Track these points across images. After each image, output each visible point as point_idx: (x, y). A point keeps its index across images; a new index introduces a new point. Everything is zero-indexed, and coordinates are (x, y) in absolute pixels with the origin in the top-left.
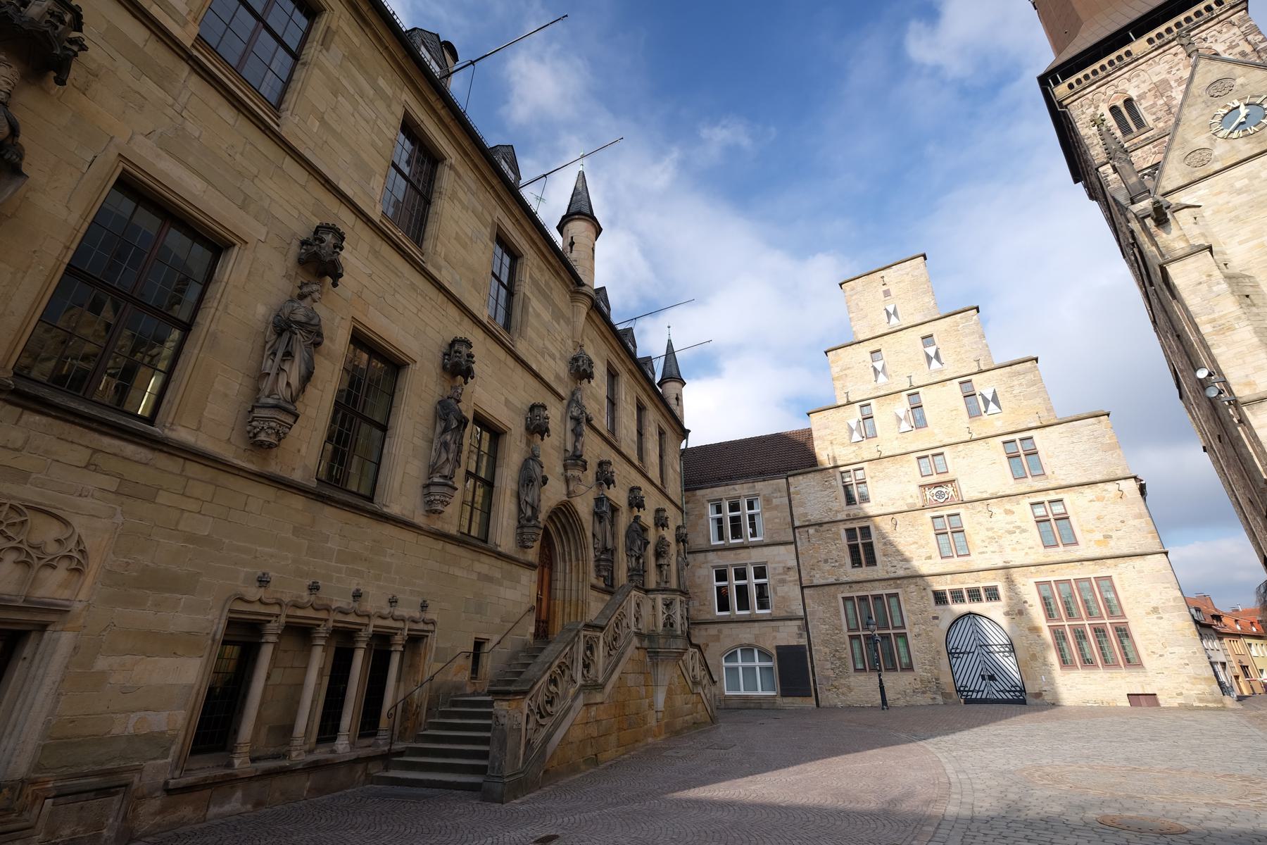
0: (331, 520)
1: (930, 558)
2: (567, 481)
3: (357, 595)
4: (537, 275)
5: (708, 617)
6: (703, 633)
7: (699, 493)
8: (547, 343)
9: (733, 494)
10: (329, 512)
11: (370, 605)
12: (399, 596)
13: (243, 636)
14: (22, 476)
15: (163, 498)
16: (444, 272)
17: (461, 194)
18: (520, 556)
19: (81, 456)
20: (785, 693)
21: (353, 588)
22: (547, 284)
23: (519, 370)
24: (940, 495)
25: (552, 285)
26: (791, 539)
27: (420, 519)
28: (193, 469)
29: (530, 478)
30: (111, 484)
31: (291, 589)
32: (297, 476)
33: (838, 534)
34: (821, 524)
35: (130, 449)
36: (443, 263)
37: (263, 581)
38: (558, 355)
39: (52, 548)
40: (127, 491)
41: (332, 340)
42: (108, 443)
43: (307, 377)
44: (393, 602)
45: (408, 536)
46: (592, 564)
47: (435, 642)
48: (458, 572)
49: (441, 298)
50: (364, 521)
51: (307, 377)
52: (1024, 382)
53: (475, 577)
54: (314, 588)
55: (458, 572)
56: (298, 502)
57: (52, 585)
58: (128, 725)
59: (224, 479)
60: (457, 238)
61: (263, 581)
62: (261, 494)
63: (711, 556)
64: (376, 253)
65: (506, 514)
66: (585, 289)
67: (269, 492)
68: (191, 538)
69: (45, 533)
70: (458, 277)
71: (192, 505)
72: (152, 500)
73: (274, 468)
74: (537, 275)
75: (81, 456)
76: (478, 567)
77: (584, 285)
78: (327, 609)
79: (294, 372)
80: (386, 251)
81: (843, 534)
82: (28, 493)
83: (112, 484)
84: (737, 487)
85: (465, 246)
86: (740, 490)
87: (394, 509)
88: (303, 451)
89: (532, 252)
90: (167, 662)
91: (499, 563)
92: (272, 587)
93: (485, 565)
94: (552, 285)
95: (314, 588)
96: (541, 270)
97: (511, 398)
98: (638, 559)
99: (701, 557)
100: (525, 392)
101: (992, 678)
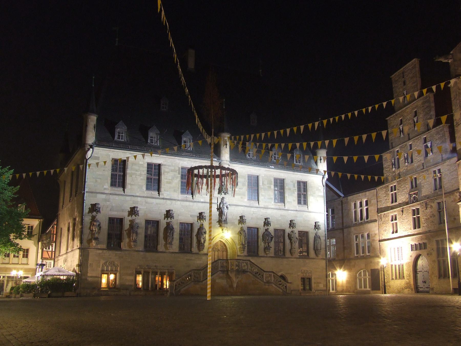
3: (156, 266)
17: (167, 170)
20: (372, 290)
58: (127, 283)
60: (167, 182)
87: (161, 250)
101: (425, 282)
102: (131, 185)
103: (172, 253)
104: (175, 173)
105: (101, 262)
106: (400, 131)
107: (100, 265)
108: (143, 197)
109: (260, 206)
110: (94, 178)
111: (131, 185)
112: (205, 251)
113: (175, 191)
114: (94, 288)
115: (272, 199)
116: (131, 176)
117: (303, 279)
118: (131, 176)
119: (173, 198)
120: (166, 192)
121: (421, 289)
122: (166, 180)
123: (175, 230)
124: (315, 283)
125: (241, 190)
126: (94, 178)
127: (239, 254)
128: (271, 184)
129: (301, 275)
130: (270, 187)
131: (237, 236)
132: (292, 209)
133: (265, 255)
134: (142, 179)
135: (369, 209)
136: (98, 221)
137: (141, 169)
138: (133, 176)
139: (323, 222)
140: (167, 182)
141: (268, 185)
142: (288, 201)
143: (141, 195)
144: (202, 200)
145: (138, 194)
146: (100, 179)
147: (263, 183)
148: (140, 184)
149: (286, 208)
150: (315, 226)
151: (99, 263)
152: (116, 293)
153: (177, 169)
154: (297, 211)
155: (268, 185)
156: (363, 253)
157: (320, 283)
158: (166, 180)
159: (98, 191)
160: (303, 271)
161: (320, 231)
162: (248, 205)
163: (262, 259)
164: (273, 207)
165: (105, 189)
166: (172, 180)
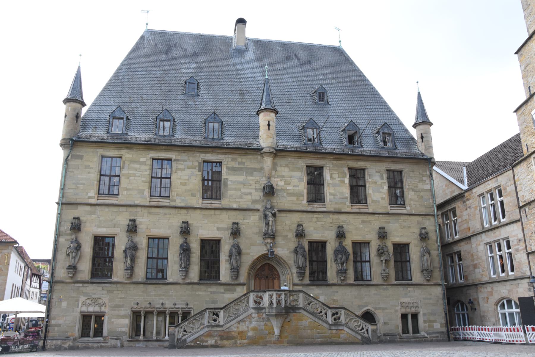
0: (151, 289)
2: (266, 245)
3: (162, 304)
4: (232, 164)
5: (486, 279)
6: (486, 290)
7: (474, 191)
8: (243, 190)
10: (150, 286)
12: (176, 303)
13: (136, 315)
14: (95, 294)
15: (114, 292)
16: (177, 201)
18: (236, 282)
19: (100, 288)
21: (161, 302)
22: (239, 163)
25: (244, 160)
26: (518, 217)
27: (181, 281)
28: (118, 285)
29: (237, 252)
30: (106, 292)
31: (144, 305)
32: (140, 280)
35: (107, 285)
36: (175, 198)
37: (138, 304)
38: (253, 191)
39: (102, 304)
40: (109, 292)
41: (141, 245)
42: (104, 285)
43: (133, 259)
44: (175, 304)
45: (178, 287)
46: (295, 275)
48: (199, 293)
49: (177, 210)
50: (160, 286)
53: (209, 293)
54: (150, 304)
55: (199, 293)
56: (141, 286)
57: (103, 309)
59: (125, 285)
60: (181, 184)
61: (138, 304)
62: (132, 286)
63: (484, 236)
64: (150, 213)
65: (224, 269)
66: (263, 151)
67: (134, 286)
68: (121, 298)
69: (100, 301)
70: (183, 198)
71: (120, 292)
72: (113, 292)
73: (134, 280)
74: (232, 164)
75: (100, 288)
77: (262, 149)
78: (154, 308)
79: (129, 260)
80: (153, 210)
82: (96, 296)
83: (106, 292)
85: (185, 184)
87: (170, 280)
88: (140, 274)
89: (226, 156)
90: (122, 320)
91: (222, 287)
92: (139, 305)
93: (214, 289)
94: (244, 160)
95: (150, 304)
96: (234, 160)
98: (342, 264)
99: (479, 237)
100: (226, 220)
102: (127, 189)
104: (194, 170)
105: (80, 299)
107: (78, 304)
110: (74, 184)
111: (127, 189)
113: (193, 195)
115: (346, 198)
116: (128, 179)
117: (404, 316)
118: (128, 179)
119: (189, 205)
120: (179, 197)
122: (179, 181)
123: (193, 250)
124: (425, 322)
125: (297, 188)
126: (74, 184)
128: (344, 177)
129: (400, 311)
130: (343, 182)
131: (292, 255)
132: (381, 211)
133: (339, 282)
134: (143, 182)
135: (505, 202)
137: (143, 167)
138: (131, 178)
140: (181, 184)
141: (339, 179)
142: (374, 201)
143: (142, 204)
144: (235, 206)
145: (137, 202)
146: (84, 184)
147: (331, 177)
148: (140, 188)
149: (370, 211)
150: (421, 234)
152: (99, 345)
153: (197, 164)
154: (388, 214)
155: (339, 179)
156: (503, 271)
157: (435, 321)
158: (179, 181)
160: (404, 304)
162: (309, 209)
163: (335, 288)
164: (349, 210)
166: (188, 180)
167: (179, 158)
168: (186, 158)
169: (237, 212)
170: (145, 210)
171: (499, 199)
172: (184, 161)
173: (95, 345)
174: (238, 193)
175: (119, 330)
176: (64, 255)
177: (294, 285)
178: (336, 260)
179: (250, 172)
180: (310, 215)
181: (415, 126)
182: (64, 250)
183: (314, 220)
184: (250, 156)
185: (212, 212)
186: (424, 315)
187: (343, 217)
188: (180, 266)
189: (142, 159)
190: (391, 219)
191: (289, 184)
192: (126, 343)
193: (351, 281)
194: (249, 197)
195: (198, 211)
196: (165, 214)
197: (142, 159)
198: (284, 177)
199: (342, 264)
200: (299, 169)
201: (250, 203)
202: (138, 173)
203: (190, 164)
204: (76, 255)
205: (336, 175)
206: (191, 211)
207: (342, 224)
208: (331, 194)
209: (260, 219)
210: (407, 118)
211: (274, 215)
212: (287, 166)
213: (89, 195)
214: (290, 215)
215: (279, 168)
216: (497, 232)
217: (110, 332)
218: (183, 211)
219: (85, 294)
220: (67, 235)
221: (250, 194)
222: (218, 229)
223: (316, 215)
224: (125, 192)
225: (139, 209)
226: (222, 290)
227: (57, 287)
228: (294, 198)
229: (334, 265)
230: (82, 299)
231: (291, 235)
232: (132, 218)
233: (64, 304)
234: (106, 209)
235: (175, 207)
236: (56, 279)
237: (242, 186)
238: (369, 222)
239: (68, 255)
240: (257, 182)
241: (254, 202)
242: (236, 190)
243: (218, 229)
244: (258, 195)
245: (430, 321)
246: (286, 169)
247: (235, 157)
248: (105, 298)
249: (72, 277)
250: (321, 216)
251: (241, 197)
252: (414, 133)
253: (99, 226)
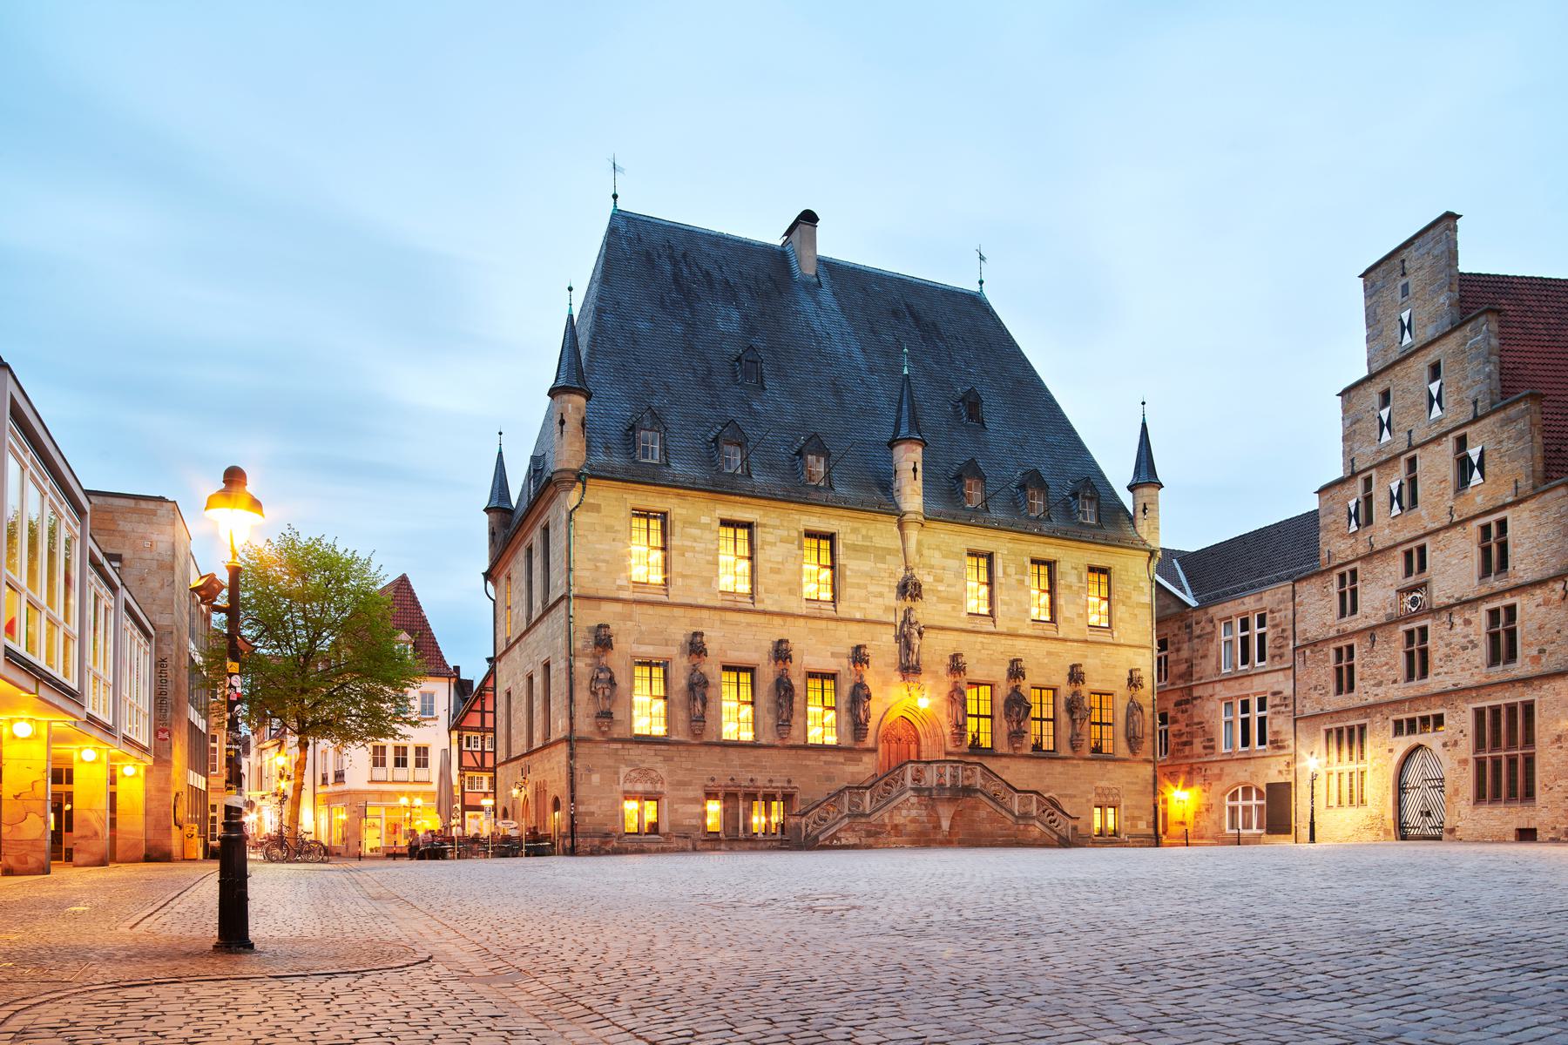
1: (1395, 682)
7: (1212, 610)
8: (871, 588)
9: (1243, 608)
11: (759, 783)
17: (770, 538)
23: (842, 625)
24: (1414, 602)
27: (778, 743)
33: (1327, 655)
34: (1315, 644)
45: (774, 752)
47: (798, 796)
51: (704, 705)
52: (1513, 433)
57: (659, 787)
60: (772, 571)
62: (703, 750)
64: (723, 622)
73: (706, 739)
76: (823, 758)
79: (699, 705)
80: (729, 616)
81: (1332, 654)
82: (645, 765)
84: (1246, 600)
86: (1249, 604)
94: (871, 533)
96: (855, 531)
97: (837, 650)
98: (1019, 722)
102: (684, 576)
103: (792, 747)
106: (1382, 426)
108: (715, 608)
109: (999, 629)
111: (684, 576)
112: (869, 742)
114: (607, 835)
119: (786, 610)
121: (1412, 832)
127: (950, 748)
136: (609, 670)
139: (1149, 669)
140: (772, 571)
144: (858, 616)
145: (701, 601)
147: (1005, 573)
149: (1061, 635)
150: (1130, 680)
151: (617, 773)
153: (795, 534)
154: (1086, 641)
159: (602, 594)
161: (1141, 692)
162: (969, 627)
164: (1029, 631)
165: (620, 588)
167: (764, 521)
168: (777, 522)
169: (863, 626)
170: (716, 615)
171: (1258, 631)
172: (774, 527)
173: (654, 847)
174: (863, 593)
175: (687, 822)
176: (587, 694)
177: (947, 753)
178: (1007, 715)
179: (881, 554)
180: (972, 637)
181: (1131, 488)
182: (586, 683)
183: (978, 646)
184: (879, 526)
185: (823, 624)
186: (1126, 807)
187: (1020, 644)
188: (778, 718)
189: (705, 520)
190: (1090, 650)
191: (939, 580)
192: (699, 845)
193: (1028, 751)
194: (880, 601)
195: (802, 622)
196: (749, 625)
197: (705, 520)
198: (932, 567)
199: (1019, 722)
200: (956, 556)
201: (880, 612)
202: (699, 546)
203: (785, 533)
204: (612, 692)
205: (1011, 570)
206: (789, 620)
207: (1018, 656)
208: (1004, 603)
209: (897, 638)
210: (1118, 471)
211: (920, 633)
212: (938, 548)
213: (619, 582)
214: (941, 635)
215: (925, 552)
216: (1247, 682)
217: (672, 825)
218: (778, 621)
219: (628, 763)
220: (586, 655)
221: (881, 595)
222: (833, 655)
223: (980, 638)
224: (679, 581)
225: (705, 614)
226: (841, 760)
227: (581, 749)
228: (948, 607)
229: (1005, 724)
230: (624, 770)
231: (943, 670)
232: (695, 629)
233: (596, 778)
234: (650, 610)
235: (765, 613)
236: (577, 734)
237: (868, 581)
238: (1057, 654)
239: (594, 693)
240: (892, 575)
241: (887, 609)
242: (858, 586)
243: (833, 655)
244: (891, 598)
245: (1134, 818)
246: (937, 554)
247: (856, 525)
248: (662, 770)
249: (604, 733)
250: (987, 639)
251: (867, 601)
252: (1127, 499)
253: (639, 642)
